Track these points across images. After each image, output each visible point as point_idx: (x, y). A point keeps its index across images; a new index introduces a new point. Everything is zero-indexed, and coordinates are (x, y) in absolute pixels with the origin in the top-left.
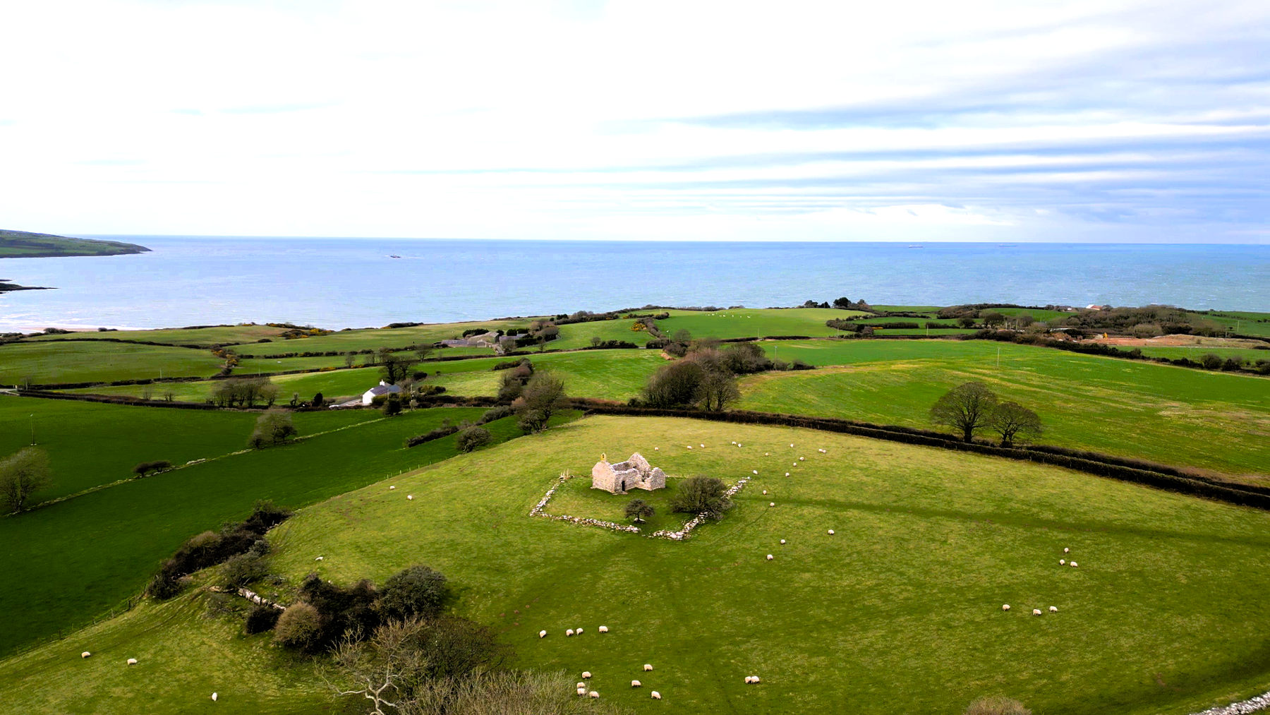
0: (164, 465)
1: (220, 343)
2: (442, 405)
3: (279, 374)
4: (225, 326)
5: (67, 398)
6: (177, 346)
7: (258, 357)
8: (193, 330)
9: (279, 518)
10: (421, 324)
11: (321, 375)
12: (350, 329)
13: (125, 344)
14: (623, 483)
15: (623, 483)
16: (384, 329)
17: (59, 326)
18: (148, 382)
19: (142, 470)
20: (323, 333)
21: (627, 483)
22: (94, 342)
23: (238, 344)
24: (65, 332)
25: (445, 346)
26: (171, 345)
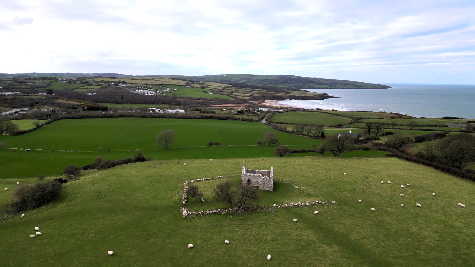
0: (220, 144)
1: (361, 117)
3: (352, 128)
4: (373, 112)
6: (345, 117)
8: (359, 112)
9: (143, 160)
10: (462, 118)
12: (424, 118)
14: (249, 181)
15: (249, 181)
16: (440, 119)
17: (320, 108)
19: (211, 144)
20: (410, 118)
21: (252, 181)
22: (320, 113)
23: (369, 118)
24: (321, 110)
25: (447, 126)
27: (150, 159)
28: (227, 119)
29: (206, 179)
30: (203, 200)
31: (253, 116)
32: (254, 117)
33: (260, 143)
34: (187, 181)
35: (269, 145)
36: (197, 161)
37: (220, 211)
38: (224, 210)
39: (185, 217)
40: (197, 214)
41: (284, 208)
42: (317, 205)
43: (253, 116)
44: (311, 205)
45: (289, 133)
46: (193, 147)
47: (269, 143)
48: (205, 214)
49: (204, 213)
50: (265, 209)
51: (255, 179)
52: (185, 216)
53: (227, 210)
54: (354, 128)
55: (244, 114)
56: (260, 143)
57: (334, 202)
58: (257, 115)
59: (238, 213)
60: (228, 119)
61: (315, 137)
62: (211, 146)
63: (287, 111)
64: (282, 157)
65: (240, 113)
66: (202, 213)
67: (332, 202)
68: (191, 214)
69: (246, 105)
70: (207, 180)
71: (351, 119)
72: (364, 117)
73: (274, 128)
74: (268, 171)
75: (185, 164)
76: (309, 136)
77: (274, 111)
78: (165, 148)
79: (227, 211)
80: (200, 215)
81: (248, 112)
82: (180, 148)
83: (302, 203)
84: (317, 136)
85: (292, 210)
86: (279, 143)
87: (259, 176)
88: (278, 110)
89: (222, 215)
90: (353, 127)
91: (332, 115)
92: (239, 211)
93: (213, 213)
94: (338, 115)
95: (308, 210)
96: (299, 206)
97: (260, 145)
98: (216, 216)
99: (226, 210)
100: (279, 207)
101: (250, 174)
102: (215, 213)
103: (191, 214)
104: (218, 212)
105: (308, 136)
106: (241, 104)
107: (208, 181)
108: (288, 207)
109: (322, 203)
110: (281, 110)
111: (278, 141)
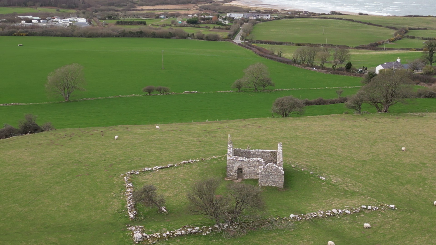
0: (165, 90)
1: (412, 27)
2: (418, 84)
3: (397, 50)
4: (432, 17)
5: (89, 36)
6: (384, 27)
7: (418, 38)
9: (36, 129)
11: (410, 53)
13: (355, 23)
14: (240, 170)
15: (240, 170)
18: (281, 43)
19: (149, 91)
21: (246, 170)
22: (338, 20)
23: (426, 29)
24: (340, 14)
26: (381, 26)
27: (49, 128)
28: (169, 36)
29: (162, 168)
30: (165, 210)
31: (217, 28)
32: (218, 31)
33: (239, 86)
34: (129, 172)
35: (256, 89)
36: (136, 129)
37: (199, 230)
38: (206, 228)
39: (139, 243)
40: (159, 238)
41: (308, 220)
42: (364, 212)
43: (217, 28)
44: (354, 213)
45: (287, 63)
46: (117, 97)
47: (255, 85)
48: (174, 236)
49: (170, 235)
50: (276, 224)
51: (250, 168)
52: (139, 242)
53: (210, 228)
54: (401, 49)
55: (201, 26)
56: (239, 86)
57: (392, 206)
58: (224, 27)
59: (232, 234)
60: (172, 37)
61: (335, 70)
62: (150, 93)
63: (279, 19)
64: (286, 116)
65: (191, 23)
66: (167, 235)
67: (388, 207)
68: (148, 237)
69: (200, 7)
70: (163, 169)
71: (394, 31)
72: (417, 28)
73: (260, 55)
74: (272, 152)
75: (116, 137)
76: (323, 68)
77: (254, 18)
78: (66, 99)
79: (211, 230)
80: (165, 239)
81: (206, 21)
82: (93, 99)
83: (338, 210)
84: (338, 70)
85: (324, 224)
86: (272, 85)
87: (259, 161)
88: (262, 15)
89: (203, 238)
90: (399, 48)
91: (360, 24)
92: (231, 228)
93: (186, 234)
94: (370, 24)
95: (350, 223)
96: (334, 216)
97: (239, 89)
98: (193, 240)
99: (208, 228)
100: (300, 220)
101: (241, 158)
102: (191, 233)
103: (149, 238)
104: (196, 232)
105: (322, 69)
106: (190, 4)
107: (165, 171)
108: (316, 219)
109: (372, 208)
110: (268, 16)
111: (272, 82)
